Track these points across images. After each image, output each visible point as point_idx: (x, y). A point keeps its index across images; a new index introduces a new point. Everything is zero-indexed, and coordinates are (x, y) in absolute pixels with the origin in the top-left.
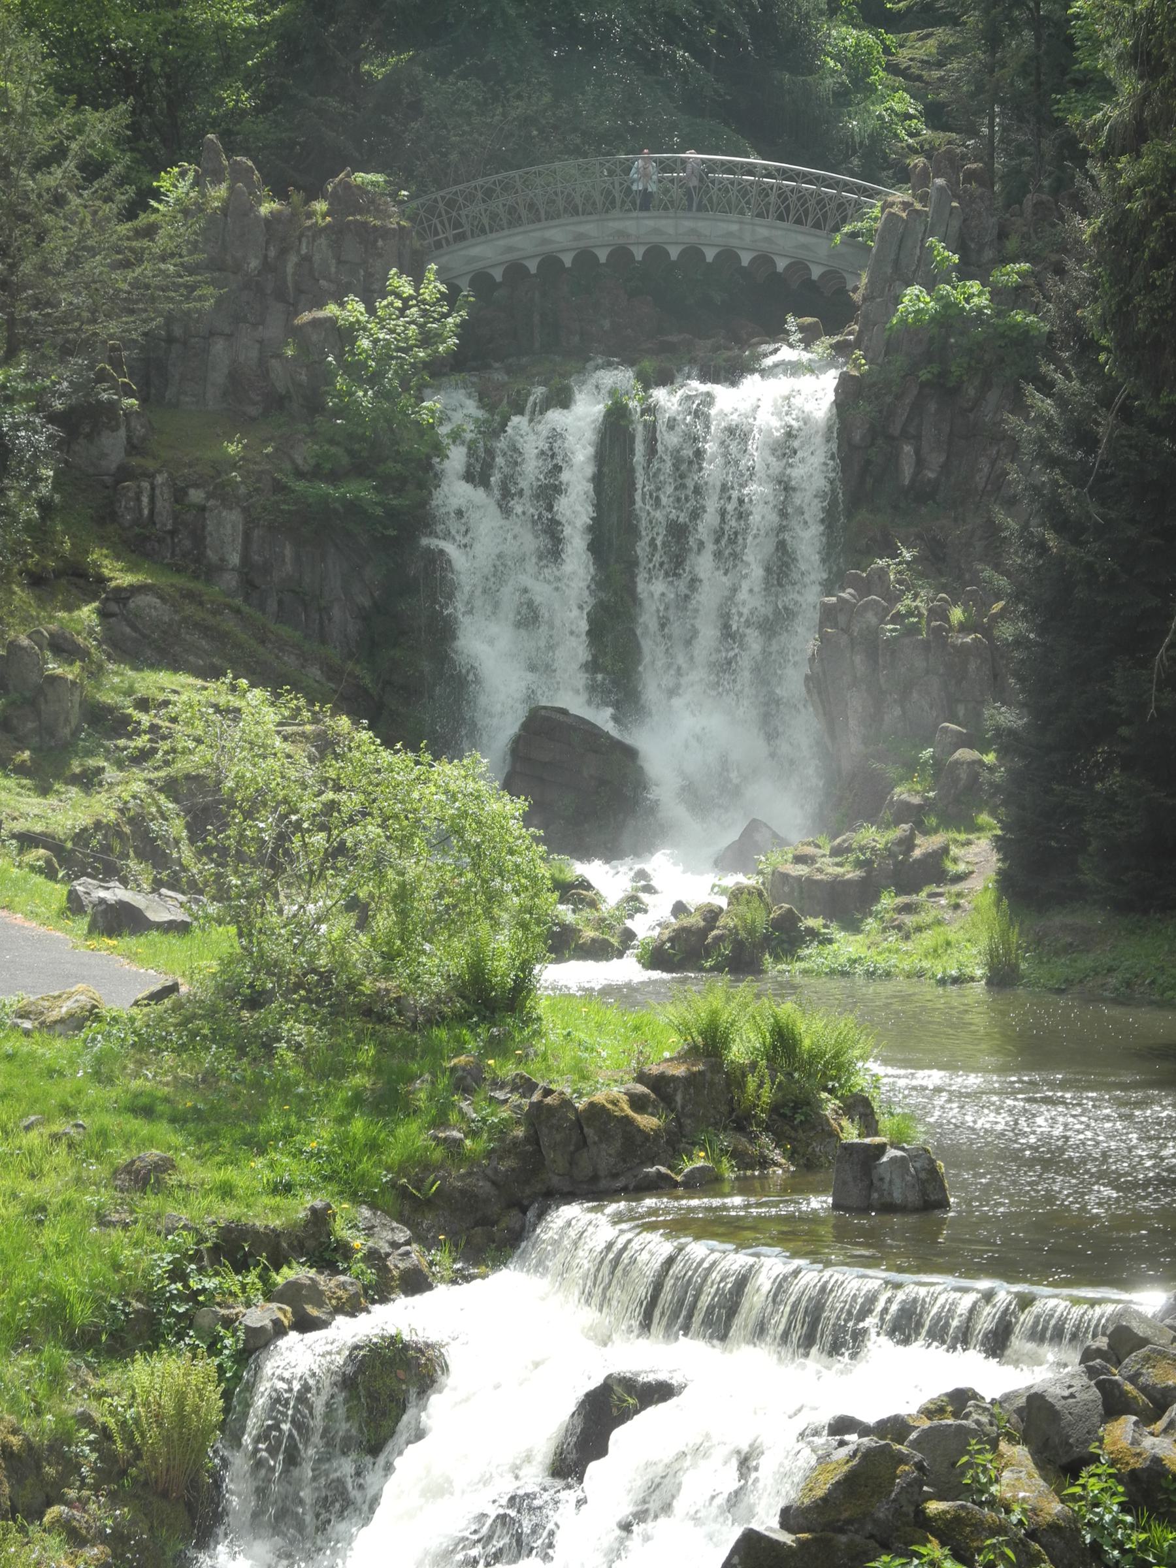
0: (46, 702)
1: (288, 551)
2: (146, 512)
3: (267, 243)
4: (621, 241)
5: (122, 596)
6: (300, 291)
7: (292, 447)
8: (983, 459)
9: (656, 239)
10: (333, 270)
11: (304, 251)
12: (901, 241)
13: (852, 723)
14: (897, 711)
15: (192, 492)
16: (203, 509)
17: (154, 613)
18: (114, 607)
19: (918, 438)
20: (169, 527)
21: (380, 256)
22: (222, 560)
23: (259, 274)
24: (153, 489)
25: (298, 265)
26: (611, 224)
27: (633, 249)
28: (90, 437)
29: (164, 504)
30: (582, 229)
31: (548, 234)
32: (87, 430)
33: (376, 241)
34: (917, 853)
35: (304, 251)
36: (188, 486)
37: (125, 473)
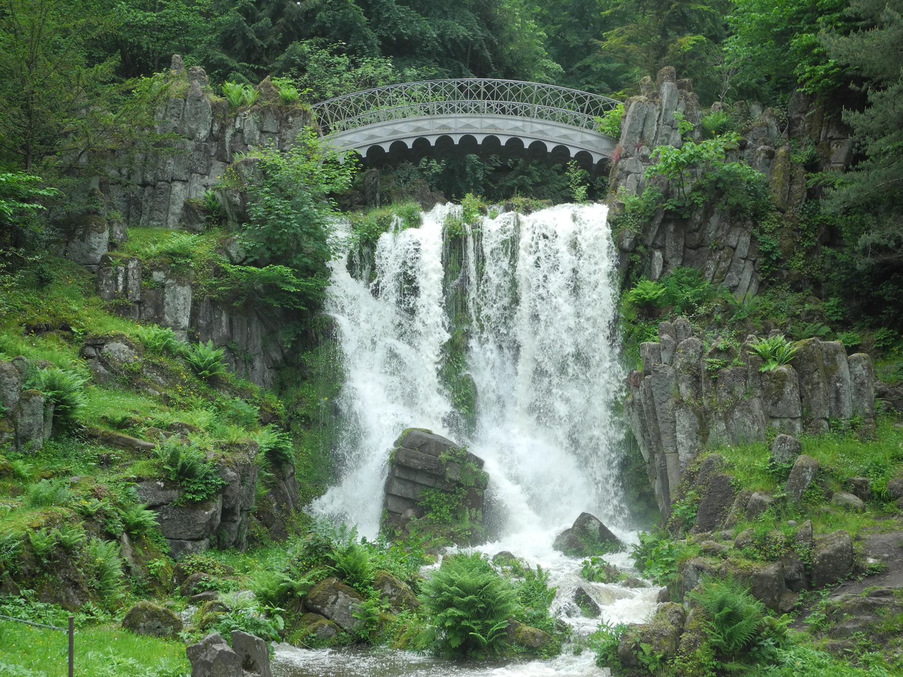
0: (22, 415)
1: (224, 318)
2: (121, 288)
3: (213, 121)
4: (445, 132)
5: (98, 343)
7: (229, 245)
8: (710, 262)
10: (257, 138)
11: (238, 126)
12: (645, 120)
13: (680, 437)
15: (155, 274)
17: (123, 356)
18: (92, 351)
20: (138, 299)
21: (290, 128)
24: (126, 269)
25: (234, 135)
26: (438, 121)
27: (453, 137)
28: (83, 239)
31: (397, 127)
32: (81, 233)
33: (287, 118)
35: (238, 126)
36: (152, 270)
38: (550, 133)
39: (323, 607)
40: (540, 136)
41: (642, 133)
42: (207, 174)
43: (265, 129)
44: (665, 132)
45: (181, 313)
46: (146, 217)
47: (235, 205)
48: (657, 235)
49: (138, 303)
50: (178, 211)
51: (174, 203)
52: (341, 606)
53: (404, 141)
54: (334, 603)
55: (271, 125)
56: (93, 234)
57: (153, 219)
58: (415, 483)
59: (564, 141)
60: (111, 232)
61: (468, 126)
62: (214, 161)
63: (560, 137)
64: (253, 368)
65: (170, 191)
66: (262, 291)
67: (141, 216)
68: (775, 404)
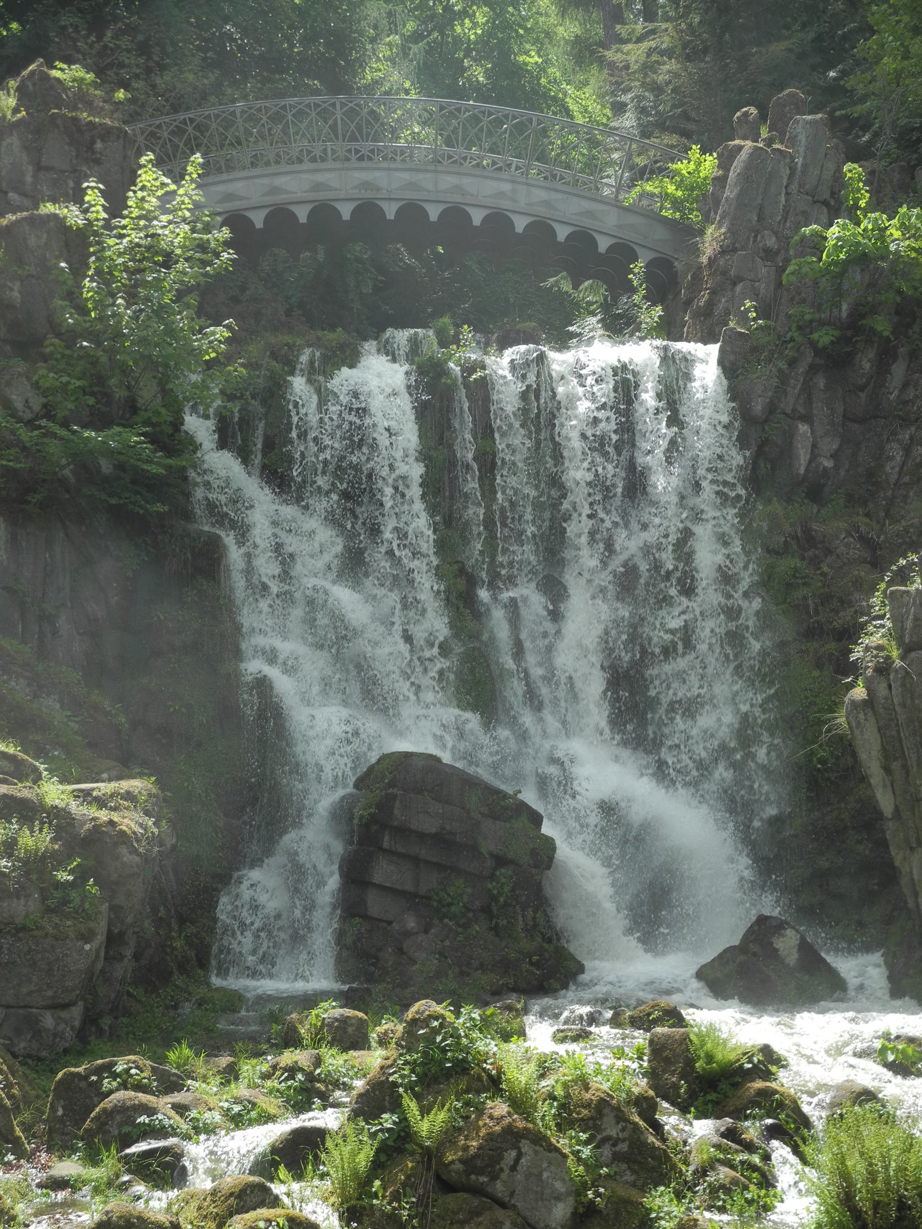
4: (370, 195)
8: (895, 445)
10: (29, 179)
21: (98, 162)
26: (356, 174)
27: (384, 205)
30: (320, 178)
31: (280, 181)
33: (93, 142)
39: (494, 1177)
41: (761, 208)
43: (45, 162)
52: (528, 1175)
53: (293, 208)
54: (513, 1168)
58: (416, 860)
59: (587, 223)
64: (55, 633)
66: (72, 479)
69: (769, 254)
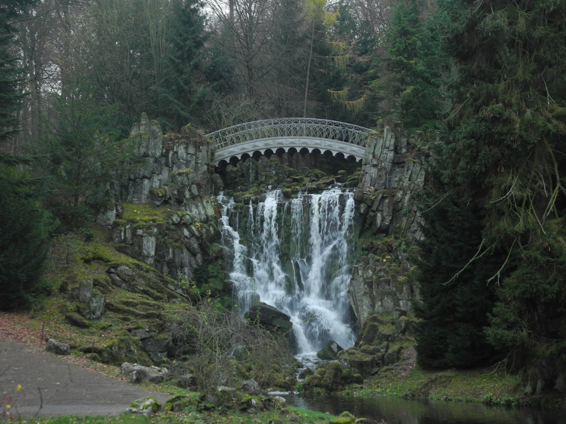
2: (123, 238)
4: (281, 146)
5: (116, 266)
6: (173, 163)
9: (292, 145)
10: (185, 156)
11: (175, 150)
14: (380, 303)
16: (142, 236)
17: (126, 272)
18: (113, 270)
19: (382, 211)
20: (130, 243)
21: (201, 151)
22: (149, 253)
23: (160, 158)
24: (125, 229)
25: (173, 155)
26: (277, 140)
28: (104, 213)
29: (129, 235)
30: (267, 142)
31: (257, 144)
33: (199, 147)
34: (390, 351)
35: (175, 150)
37: (116, 225)
38: (334, 146)
40: (329, 148)
41: (374, 153)
42: (160, 174)
44: (385, 152)
45: (150, 249)
46: (131, 196)
47: (175, 195)
48: (379, 205)
49: (131, 244)
50: (146, 193)
51: (144, 189)
55: (191, 150)
56: (109, 211)
57: (134, 198)
59: (341, 150)
60: (117, 210)
61: (293, 143)
62: (163, 166)
63: (339, 148)
65: (142, 183)
67: (128, 195)
68: (400, 294)
69: (375, 166)
